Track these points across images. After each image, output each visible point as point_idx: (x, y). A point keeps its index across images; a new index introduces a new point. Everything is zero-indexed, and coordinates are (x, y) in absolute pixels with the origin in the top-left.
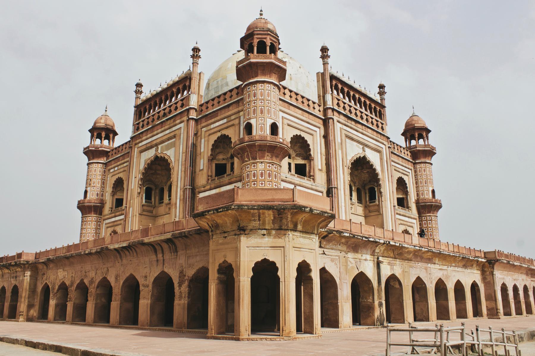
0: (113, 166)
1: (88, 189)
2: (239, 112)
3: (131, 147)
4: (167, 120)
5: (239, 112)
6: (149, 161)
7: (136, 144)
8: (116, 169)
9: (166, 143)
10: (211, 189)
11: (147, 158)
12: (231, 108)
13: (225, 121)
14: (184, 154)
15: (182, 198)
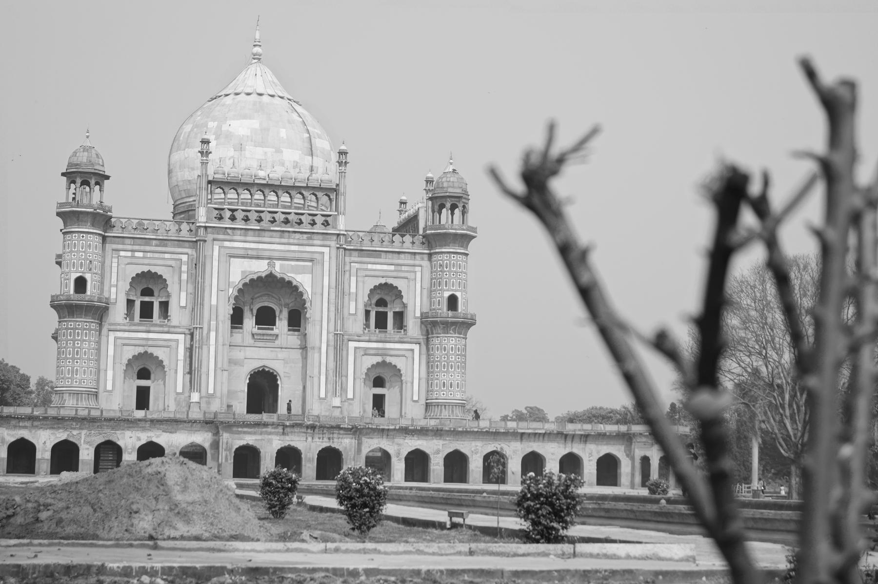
0: (129, 247)
1: (88, 276)
2: (414, 266)
3: (205, 241)
4: (295, 232)
5: (414, 266)
6: (255, 277)
7: (214, 240)
8: (137, 254)
9: (293, 263)
10: (369, 341)
11: (249, 269)
12: (402, 256)
13: (392, 268)
14: (333, 291)
15: (332, 343)
